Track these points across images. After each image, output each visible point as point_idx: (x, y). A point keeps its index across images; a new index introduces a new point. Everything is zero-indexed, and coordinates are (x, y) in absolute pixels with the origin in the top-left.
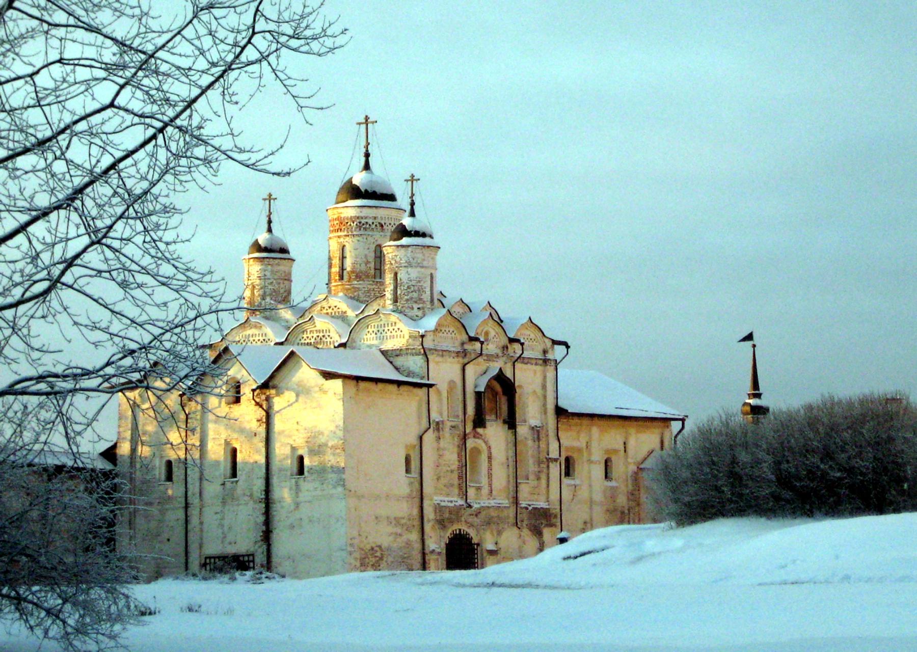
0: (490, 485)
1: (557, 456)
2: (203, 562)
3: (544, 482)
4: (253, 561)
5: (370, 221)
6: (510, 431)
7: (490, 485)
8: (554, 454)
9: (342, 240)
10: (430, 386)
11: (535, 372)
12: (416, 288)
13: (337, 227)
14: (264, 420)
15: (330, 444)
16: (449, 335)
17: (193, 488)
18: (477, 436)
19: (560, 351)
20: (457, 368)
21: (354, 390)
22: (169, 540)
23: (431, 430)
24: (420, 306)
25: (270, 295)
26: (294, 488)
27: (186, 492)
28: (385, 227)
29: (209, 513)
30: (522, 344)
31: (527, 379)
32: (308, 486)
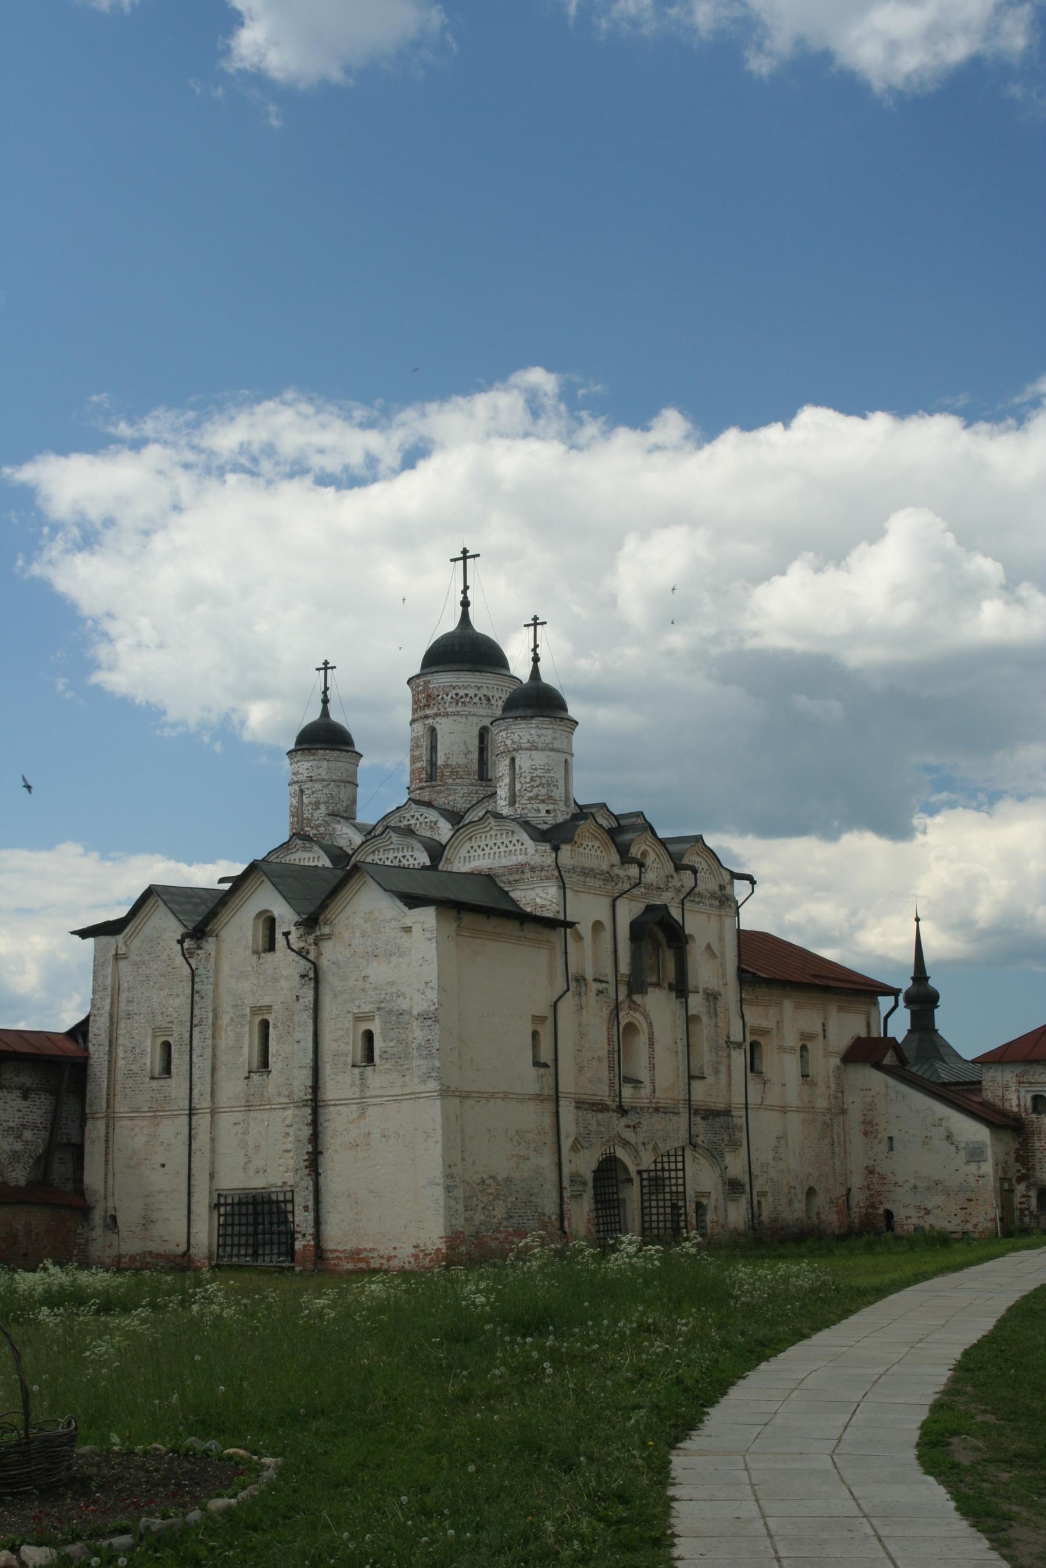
0: (653, 1082)
1: (741, 1039)
2: (216, 1201)
3: (723, 1076)
4: (292, 1201)
5: (471, 692)
6: (679, 1000)
7: (653, 1082)
8: (737, 1036)
9: (430, 721)
10: (571, 925)
12: (544, 781)
13: (424, 701)
14: (312, 975)
15: (415, 1013)
17: (202, 1087)
18: (633, 1006)
20: (605, 903)
21: (454, 925)
22: (163, 1165)
23: (569, 993)
24: (550, 807)
25: (326, 803)
26: (358, 1082)
27: (191, 1089)
28: (493, 702)
29: (225, 1121)
30: (695, 872)
31: (698, 925)
32: (378, 1079)
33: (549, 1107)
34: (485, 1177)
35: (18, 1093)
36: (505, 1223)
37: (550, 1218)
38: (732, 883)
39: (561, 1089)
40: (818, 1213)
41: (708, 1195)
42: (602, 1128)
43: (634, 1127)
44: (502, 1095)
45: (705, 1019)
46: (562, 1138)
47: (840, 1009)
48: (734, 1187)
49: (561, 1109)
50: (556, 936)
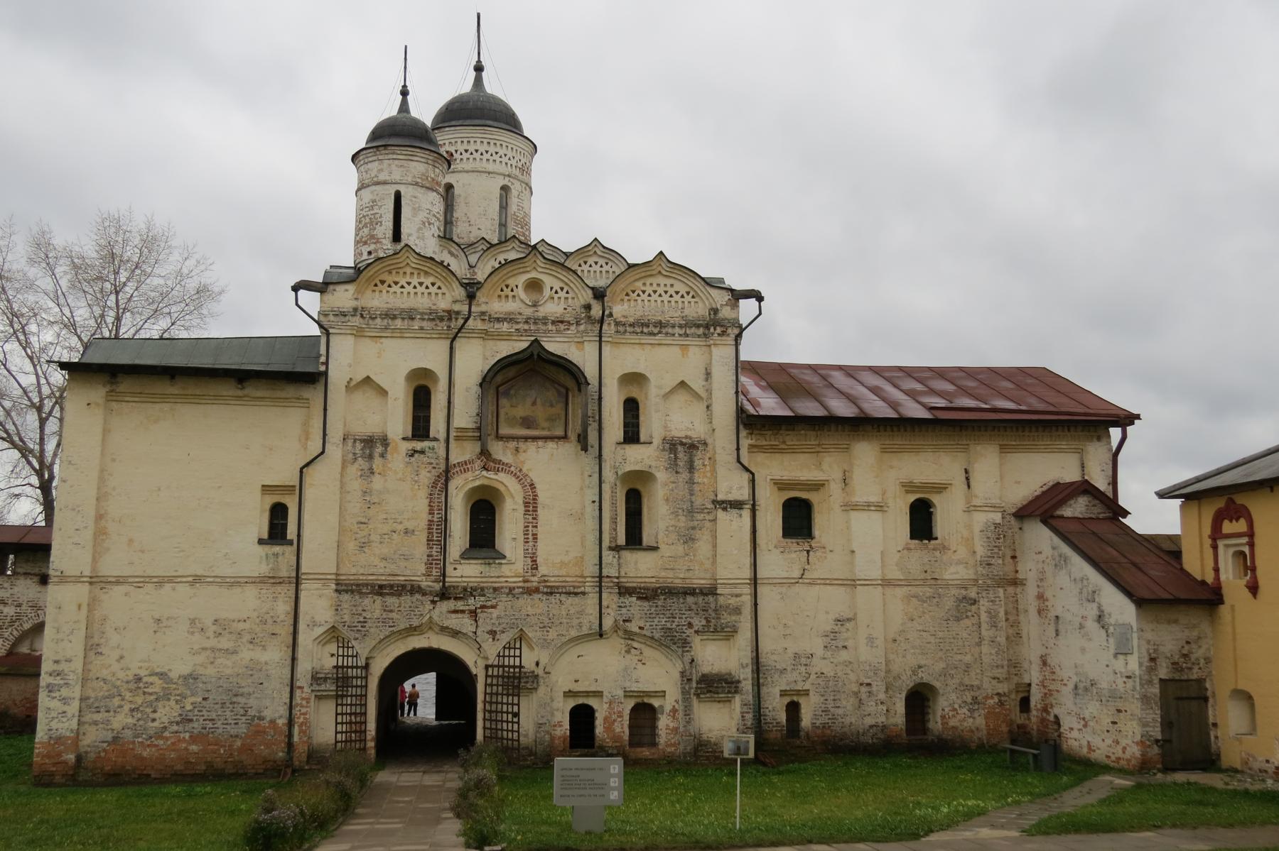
16: (420, 289)
19: (747, 308)
24: (372, 247)
34: (142, 673)
35: (36, 579)
36: (175, 728)
37: (273, 722)
38: (735, 305)
39: (303, 569)
40: (943, 717)
41: (662, 694)
43: (475, 612)
44: (190, 579)
45: (661, 476)
46: (302, 626)
47: (1004, 449)
48: (714, 686)
49: (303, 595)
50: (313, 395)
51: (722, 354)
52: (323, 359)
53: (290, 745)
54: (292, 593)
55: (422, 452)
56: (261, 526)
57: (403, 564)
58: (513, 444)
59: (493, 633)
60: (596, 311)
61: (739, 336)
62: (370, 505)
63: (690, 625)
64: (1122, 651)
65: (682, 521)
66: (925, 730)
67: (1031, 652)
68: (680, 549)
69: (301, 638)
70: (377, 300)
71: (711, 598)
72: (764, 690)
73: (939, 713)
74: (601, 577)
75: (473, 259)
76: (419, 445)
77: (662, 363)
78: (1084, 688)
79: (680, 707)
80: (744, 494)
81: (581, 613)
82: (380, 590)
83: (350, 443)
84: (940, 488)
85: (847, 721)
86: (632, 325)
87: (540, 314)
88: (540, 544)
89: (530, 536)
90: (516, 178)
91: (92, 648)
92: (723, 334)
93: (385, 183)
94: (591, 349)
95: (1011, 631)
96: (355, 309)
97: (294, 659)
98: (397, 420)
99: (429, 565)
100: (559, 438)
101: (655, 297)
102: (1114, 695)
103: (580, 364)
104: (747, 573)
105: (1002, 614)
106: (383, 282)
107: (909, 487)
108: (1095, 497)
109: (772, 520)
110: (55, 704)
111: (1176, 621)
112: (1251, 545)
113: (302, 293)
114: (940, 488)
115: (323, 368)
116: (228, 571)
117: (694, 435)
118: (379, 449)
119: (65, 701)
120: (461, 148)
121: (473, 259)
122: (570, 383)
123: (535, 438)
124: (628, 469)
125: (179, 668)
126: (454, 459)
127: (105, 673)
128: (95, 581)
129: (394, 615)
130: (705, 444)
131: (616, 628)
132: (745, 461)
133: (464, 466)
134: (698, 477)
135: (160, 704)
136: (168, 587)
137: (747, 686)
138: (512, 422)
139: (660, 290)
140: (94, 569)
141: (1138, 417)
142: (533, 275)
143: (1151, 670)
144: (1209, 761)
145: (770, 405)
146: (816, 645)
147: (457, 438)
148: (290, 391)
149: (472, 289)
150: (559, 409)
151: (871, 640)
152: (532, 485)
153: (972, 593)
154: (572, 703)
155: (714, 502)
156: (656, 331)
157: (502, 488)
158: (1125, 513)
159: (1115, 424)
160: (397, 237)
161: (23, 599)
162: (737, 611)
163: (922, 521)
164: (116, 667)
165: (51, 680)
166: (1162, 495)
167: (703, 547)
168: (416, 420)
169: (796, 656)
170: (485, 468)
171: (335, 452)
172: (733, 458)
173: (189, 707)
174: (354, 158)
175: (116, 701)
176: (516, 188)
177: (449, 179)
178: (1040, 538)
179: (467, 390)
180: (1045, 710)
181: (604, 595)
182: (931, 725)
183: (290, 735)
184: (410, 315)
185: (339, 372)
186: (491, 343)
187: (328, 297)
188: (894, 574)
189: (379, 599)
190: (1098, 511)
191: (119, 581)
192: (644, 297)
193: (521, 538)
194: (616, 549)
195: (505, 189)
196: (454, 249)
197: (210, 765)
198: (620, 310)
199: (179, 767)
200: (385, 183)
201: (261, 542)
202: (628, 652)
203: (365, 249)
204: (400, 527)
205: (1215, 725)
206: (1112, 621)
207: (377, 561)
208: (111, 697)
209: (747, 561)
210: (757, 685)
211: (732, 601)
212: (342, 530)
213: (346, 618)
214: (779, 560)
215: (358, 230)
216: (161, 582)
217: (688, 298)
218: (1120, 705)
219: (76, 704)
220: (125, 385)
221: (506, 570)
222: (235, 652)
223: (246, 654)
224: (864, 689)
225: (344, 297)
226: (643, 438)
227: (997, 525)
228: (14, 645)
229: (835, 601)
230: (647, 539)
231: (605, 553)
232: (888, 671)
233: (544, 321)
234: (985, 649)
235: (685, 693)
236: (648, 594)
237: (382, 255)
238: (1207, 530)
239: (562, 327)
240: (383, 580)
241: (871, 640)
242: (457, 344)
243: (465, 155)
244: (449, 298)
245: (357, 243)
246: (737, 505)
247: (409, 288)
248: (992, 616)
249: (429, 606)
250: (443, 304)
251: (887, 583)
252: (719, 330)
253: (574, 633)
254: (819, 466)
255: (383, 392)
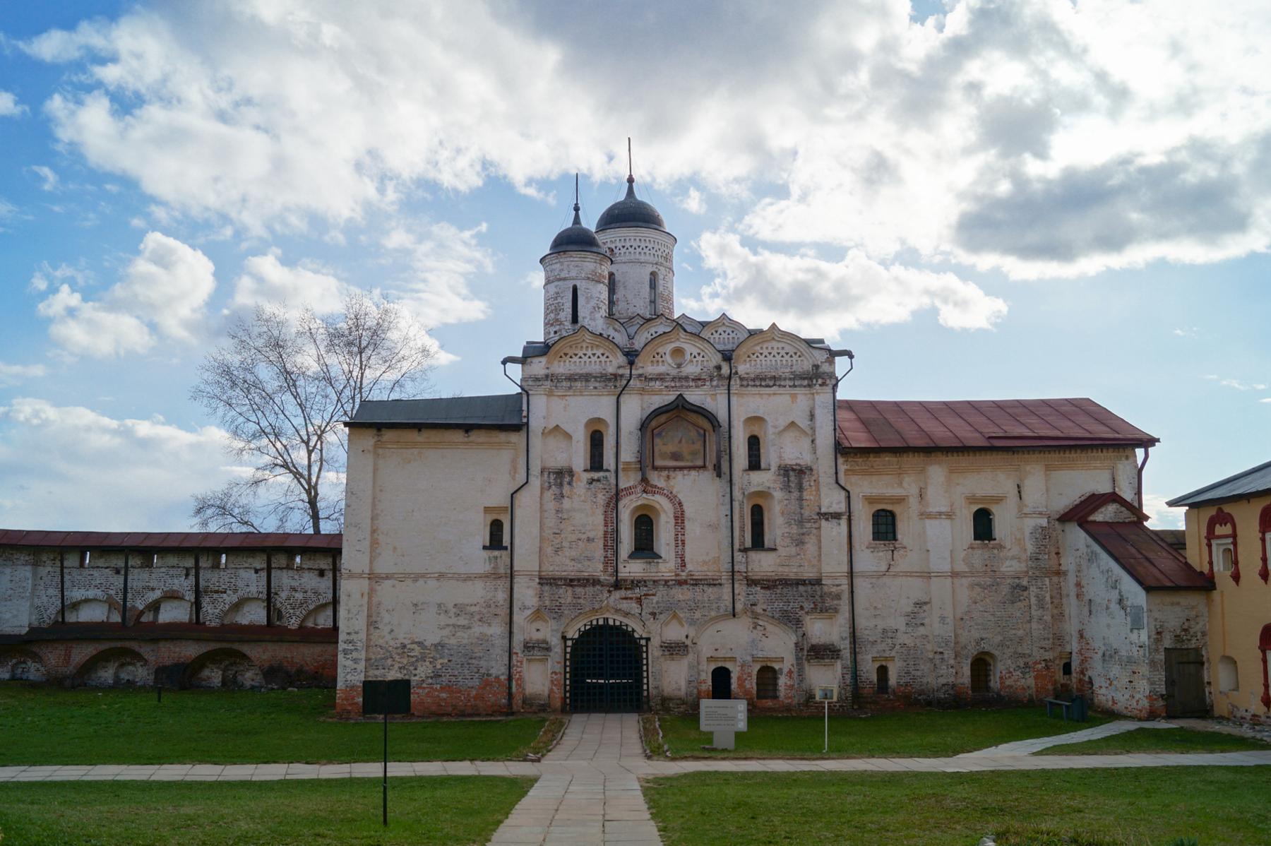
11: (794, 396)
16: (594, 359)
24: (557, 328)
33: (503, 584)
34: (406, 642)
37: (497, 677)
38: (832, 363)
40: (1001, 678)
42: (581, 601)
45: (778, 495)
46: (516, 609)
48: (822, 653)
50: (517, 438)
51: (822, 398)
52: (525, 413)
53: (510, 695)
54: (508, 585)
55: (598, 480)
56: (484, 536)
57: (586, 563)
58: (665, 473)
59: (653, 614)
60: (725, 370)
61: (835, 386)
62: (562, 520)
63: (802, 608)
64: (1136, 626)
65: (795, 530)
66: (988, 688)
67: (1071, 627)
68: (793, 550)
69: (515, 617)
70: (561, 368)
71: (817, 588)
72: (859, 657)
73: (998, 675)
74: (733, 571)
75: (632, 330)
76: (596, 475)
77: (777, 408)
78: (1110, 656)
79: (795, 670)
80: (842, 507)
81: (719, 599)
82: (571, 582)
83: (546, 474)
84: (998, 500)
85: (925, 680)
86: (753, 380)
87: (684, 374)
88: (687, 547)
89: (680, 542)
90: (661, 264)
91: (372, 624)
92: (823, 384)
93: (565, 279)
94: (722, 400)
95: (1055, 611)
96: (547, 376)
97: (511, 633)
98: (579, 457)
99: (606, 563)
100: (700, 467)
101: (770, 357)
102: (1130, 661)
103: (714, 412)
104: (845, 568)
105: (1048, 598)
106: (566, 354)
107: (972, 499)
108: (1122, 505)
109: (864, 528)
110: (349, 663)
111: (1178, 604)
112: (1235, 544)
113: (508, 365)
114: (998, 500)
115: (525, 420)
116: (463, 570)
117: (802, 462)
118: (567, 479)
119: (356, 661)
120: (619, 245)
121: (632, 330)
122: (707, 425)
123: (681, 468)
124: (753, 490)
125: (432, 639)
126: (622, 485)
127: (381, 642)
128: (374, 577)
129: (581, 601)
130: (811, 470)
131: (745, 611)
132: (842, 482)
133: (629, 491)
134: (806, 495)
135: (419, 664)
136: (421, 581)
137: (846, 653)
138: (663, 456)
139: (774, 352)
140: (371, 569)
141: (1158, 440)
142: (677, 344)
143: (1158, 641)
144: (1205, 712)
145: (859, 439)
146: (900, 623)
147: (624, 470)
148: (502, 437)
149: (631, 356)
150: (699, 446)
151: (943, 619)
152: (680, 504)
153: (1025, 583)
154: (713, 666)
155: (819, 514)
156: (771, 383)
157: (658, 507)
158: (1147, 518)
159: (1139, 446)
160: (575, 319)
161: (308, 587)
162: (838, 597)
163: (983, 525)
164: (388, 637)
165: (345, 646)
166: (1173, 503)
167: (810, 548)
168: (592, 457)
169: (884, 631)
170: (645, 491)
171: (536, 482)
172: (833, 480)
173: (439, 666)
174: (541, 261)
175: (389, 662)
176: (662, 272)
177: (613, 269)
178: (1077, 537)
179: (630, 433)
180: (1082, 673)
181: (736, 586)
182: (992, 684)
183: (510, 688)
184: (586, 378)
185: (537, 422)
186: (646, 397)
187: (526, 367)
188: (961, 567)
189: (570, 589)
190: (1126, 515)
191: (388, 577)
192: (762, 358)
193: (673, 543)
194: (745, 550)
195: (653, 274)
196: (617, 326)
197: (455, 707)
198: (742, 369)
199: (434, 708)
200: (565, 279)
201: (485, 548)
202: (755, 628)
203: (552, 329)
204: (584, 537)
205: (1209, 683)
206: (1129, 603)
207: (568, 562)
208: (386, 658)
209: (845, 559)
210: (854, 653)
211: (834, 589)
212: (542, 539)
213: (547, 603)
214: (869, 559)
215: (546, 315)
216: (416, 578)
217: (795, 357)
218: (1134, 668)
219: (363, 663)
220: (388, 435)
221: (662, 567)
222: (469, 628)
223: (477, 629)
224: (938, 656)
225: (539, 366)
226: (763, 465)
227: (1043, 528)
228: (303, 621)
229: (915, 589)
230: (767, 544)
231: (736, 554)
232: (956, 643)
233: (686, 378)
234: (1034, 625)
235: (798, 658)
236: (769, 584)
237: (565, 334)
238: (1204, 532)
239: (700, 383)
240: (573, 575)
241: (943, 619)
242: (622, 399)
243: (623, 250)
244: (615, 363)
245: (546, 324)
246: (837, 516)
247: (585, 358)
248: (1040, 600)
249: (606, 595)
250: (611, 370)
251: (954, 574)
252: (820, 381)
253: (713, 614)
254: (900, 485)
255: (568, 436)
